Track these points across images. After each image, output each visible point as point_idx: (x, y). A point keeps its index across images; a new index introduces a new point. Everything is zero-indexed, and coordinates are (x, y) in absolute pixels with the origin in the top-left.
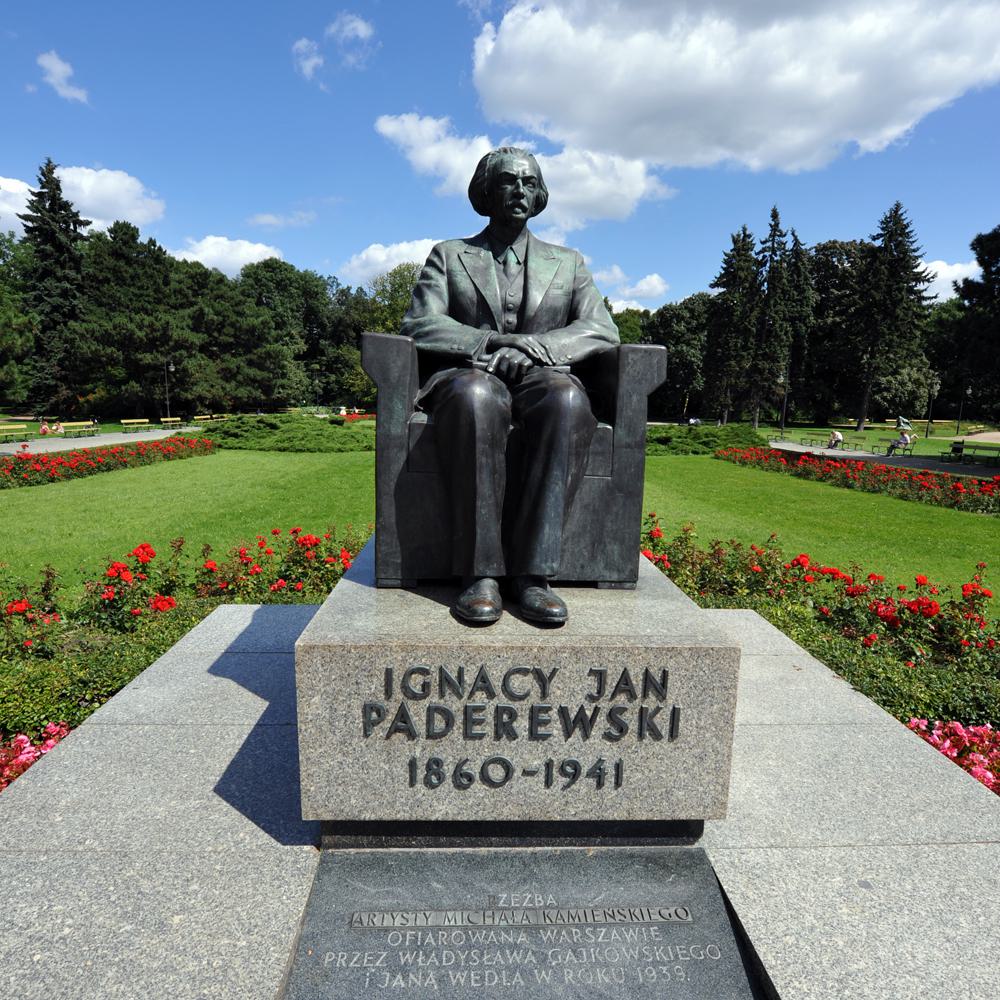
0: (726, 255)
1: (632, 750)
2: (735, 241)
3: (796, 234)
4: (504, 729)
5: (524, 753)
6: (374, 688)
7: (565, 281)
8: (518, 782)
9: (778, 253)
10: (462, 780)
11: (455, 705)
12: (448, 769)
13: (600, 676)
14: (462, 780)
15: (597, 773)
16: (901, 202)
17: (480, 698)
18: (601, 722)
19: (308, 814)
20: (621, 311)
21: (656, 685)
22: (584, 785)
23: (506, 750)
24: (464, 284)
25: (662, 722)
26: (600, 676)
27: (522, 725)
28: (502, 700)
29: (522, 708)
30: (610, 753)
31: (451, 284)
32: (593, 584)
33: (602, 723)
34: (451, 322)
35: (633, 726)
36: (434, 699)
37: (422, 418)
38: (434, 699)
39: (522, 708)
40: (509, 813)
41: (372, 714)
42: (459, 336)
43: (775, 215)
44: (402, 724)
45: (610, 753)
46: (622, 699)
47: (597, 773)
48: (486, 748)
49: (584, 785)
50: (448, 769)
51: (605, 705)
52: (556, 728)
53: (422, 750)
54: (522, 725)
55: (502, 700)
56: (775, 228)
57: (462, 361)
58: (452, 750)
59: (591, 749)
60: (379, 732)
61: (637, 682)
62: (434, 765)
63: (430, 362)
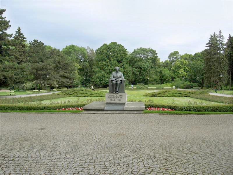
4: (115, 98)
5: (116, 99)
6: (109, 96)
7: (121, 75)
8: (116, 101)
10: (113, 100)
11: (113, 97)
14: (113, 100)
21: (122, 96)
24: (114, 75)
34: (113, 78)
37: (111, 84)
40: (115, 102)
42: (114, 79)
44: (110, 98)
48: (114, 99)
57: (113, 80)
59: (119, 99)
62: (112, 100)
63: (112, 80)
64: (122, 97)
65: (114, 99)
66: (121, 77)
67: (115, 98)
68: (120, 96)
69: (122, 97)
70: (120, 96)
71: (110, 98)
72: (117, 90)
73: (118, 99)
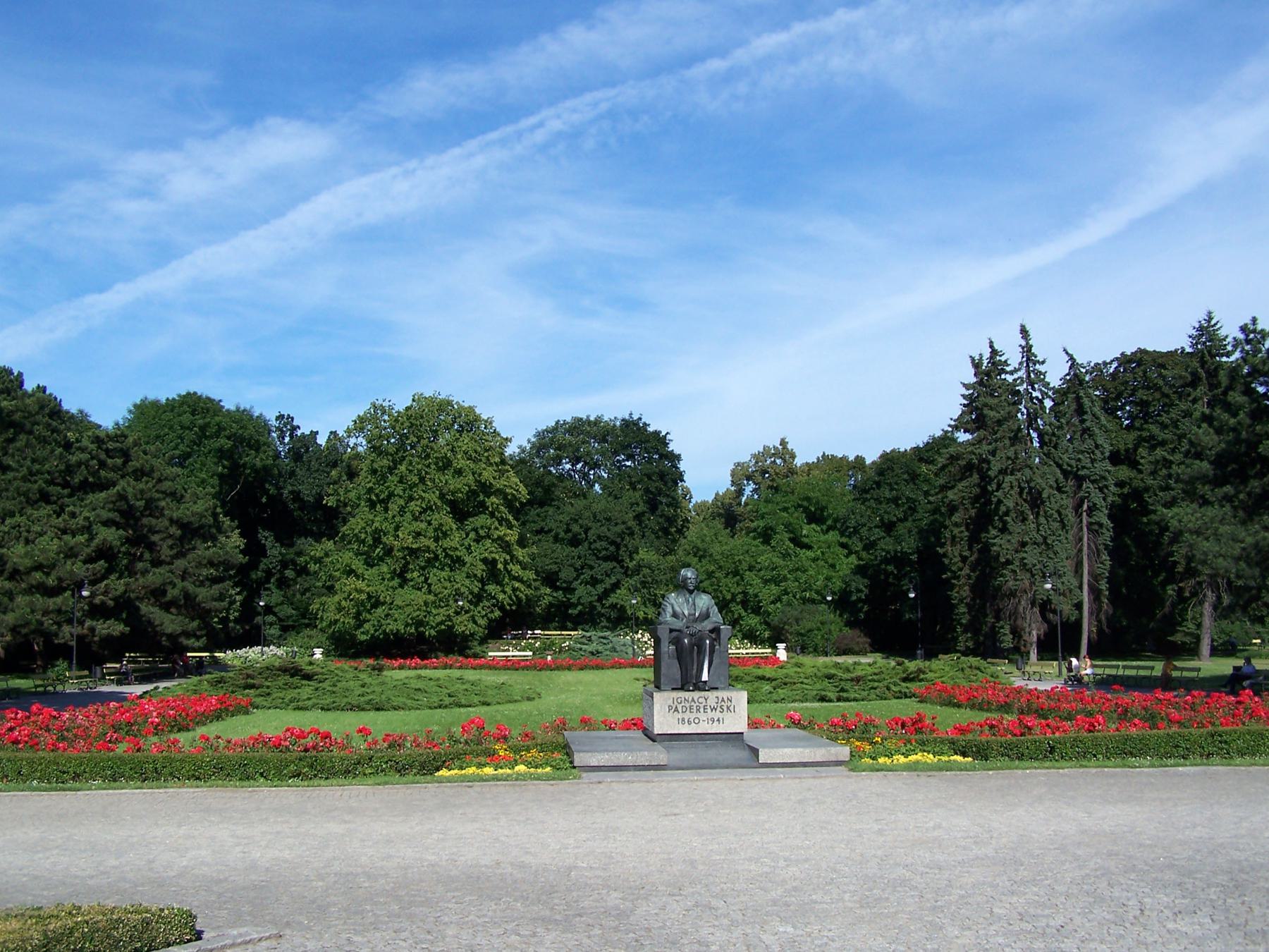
0: (966, 386)
1: (726, 715)
2: (976, 365)
3: (1070, 352)
5: (702, 716)
6: (670, 702)
9: (1036, 386)
11: (688, 705)
12: (686, 721)
13: (717, 697)
15: (718, 720)
16: (1212, 310)
17: (693, 704)
18: (719, 709)
19: (657, 730)
20: (812, 459)
22: (716, 723)
23: (698, 715)
24: (677, 609)
25: (732, 708)
26: (717, 697)
27: (702, 710)
28: (697, 704)
29: (702, 706)
30: (721, 716)
31: (673, 608)
32: (717, 688)
33: (719, 709)
35: (725, 709)
36: (683, 704)
38: (683, 704)
39: (702, 706)
41: (670, 707)
42: (678, 624)
43: (1024, 332)
45: (721, 716)
46: (723, 703)
47: (718, 720)
49: (716, 723)
50: (686, 721)
51: (719, 705)
52: (709, 710)
53: (680, 716)
54: (702, 710)
55: (697, 704)
56: (1027, 350)
58: (687, 716)
59: (717, 715)
60: (672, 711)
61: (726, 700)
62: (683, 720)
64: (728, 708)
65: (692, 716)
66: (706, 616)
67: (698, 710)
68: (723, 700)
69: (728, 708)
70: (723, 700)
71: (676, 710)
72: (705, 677)
73: (711, 714)
